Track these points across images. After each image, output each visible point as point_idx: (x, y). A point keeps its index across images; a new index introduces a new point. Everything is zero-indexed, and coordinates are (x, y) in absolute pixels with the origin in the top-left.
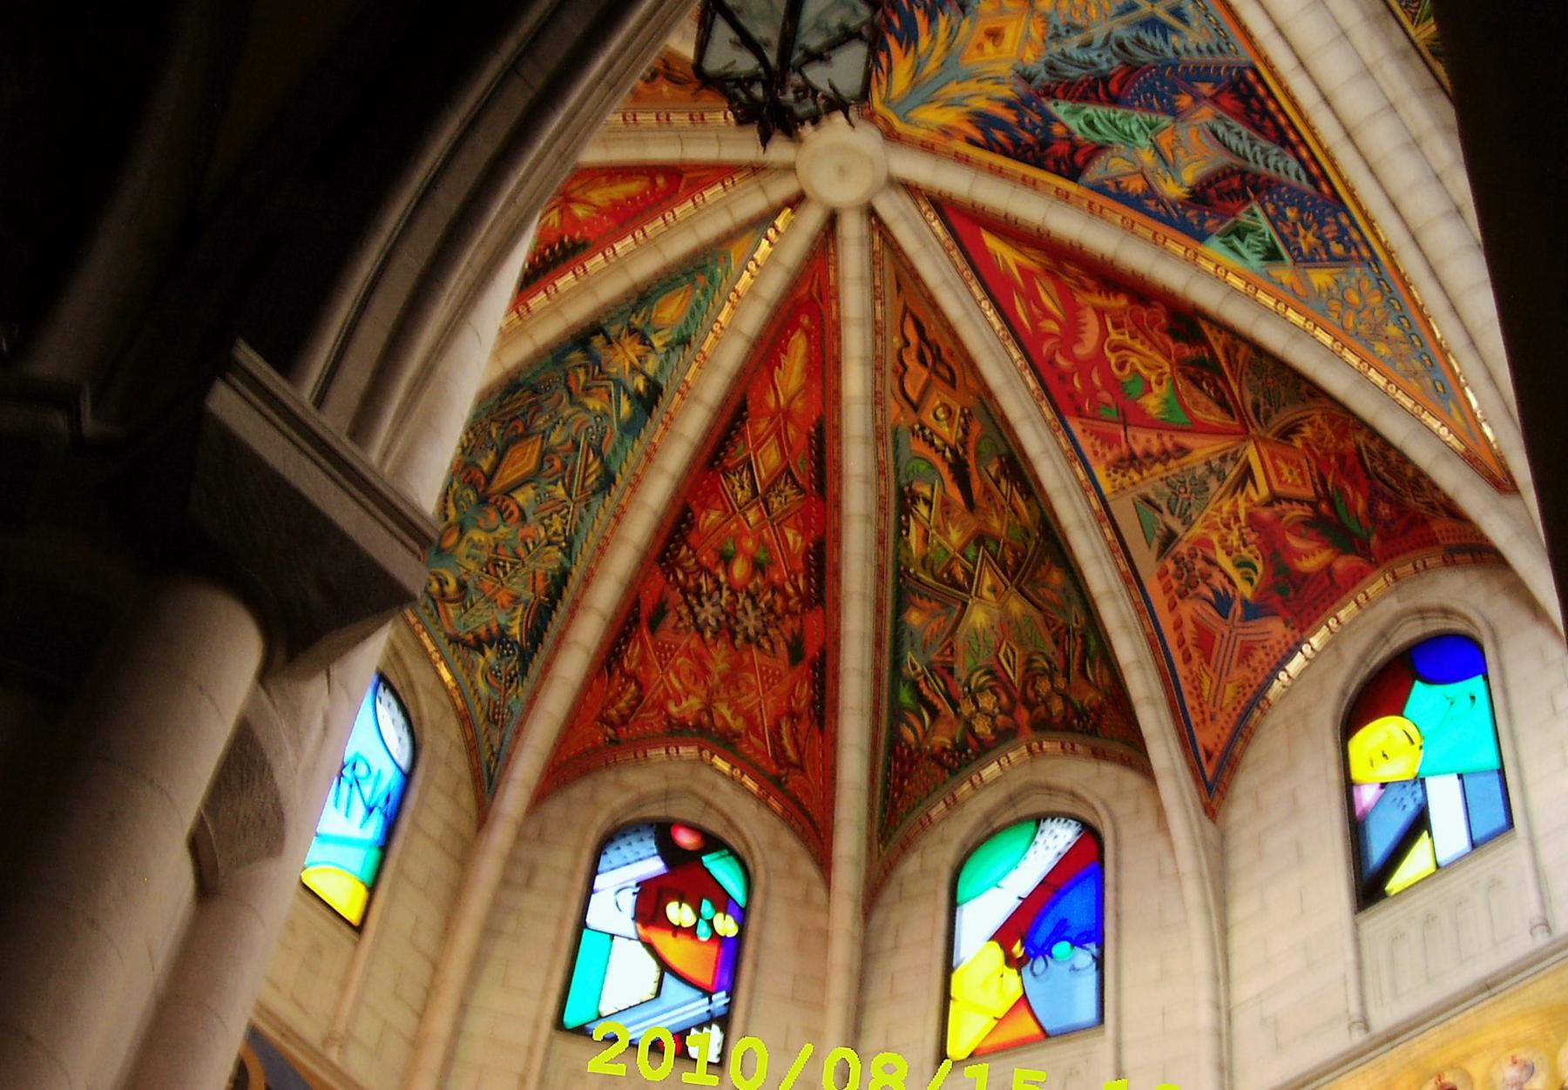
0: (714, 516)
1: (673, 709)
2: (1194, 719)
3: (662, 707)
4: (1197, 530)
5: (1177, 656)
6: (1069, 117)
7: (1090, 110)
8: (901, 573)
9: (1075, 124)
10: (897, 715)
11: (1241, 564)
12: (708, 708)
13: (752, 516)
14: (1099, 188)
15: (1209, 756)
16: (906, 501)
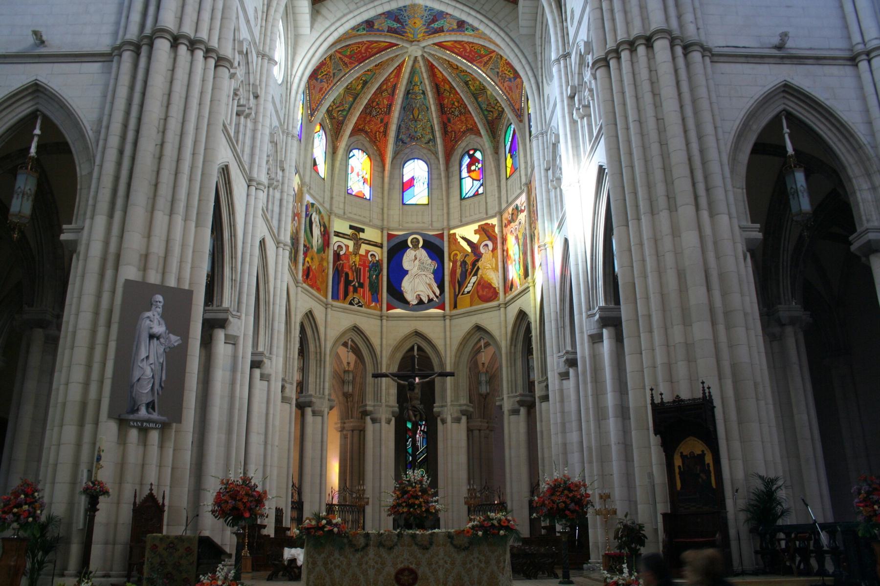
0: (446, 100)
1: (462, 130)
2: (514, 104)
3: (459, 131)
4: (501, 69)
5: (507, 94)
6: (435, 25)
7: (436, 23)
8: (473, 94)
9: (436, 26)
10: (486, 117)
11: (509, 72)
12: (467, 126)
13: (452, 95)
14: (447, 31)
15: (518, 110)
16: (466, 83)
